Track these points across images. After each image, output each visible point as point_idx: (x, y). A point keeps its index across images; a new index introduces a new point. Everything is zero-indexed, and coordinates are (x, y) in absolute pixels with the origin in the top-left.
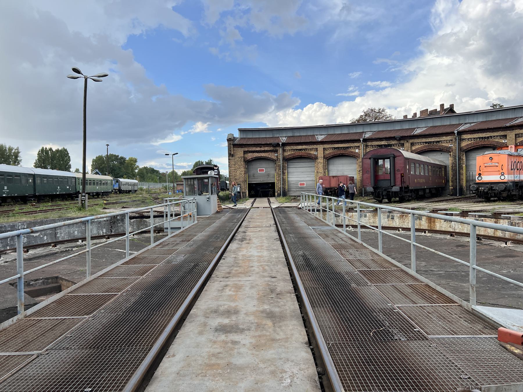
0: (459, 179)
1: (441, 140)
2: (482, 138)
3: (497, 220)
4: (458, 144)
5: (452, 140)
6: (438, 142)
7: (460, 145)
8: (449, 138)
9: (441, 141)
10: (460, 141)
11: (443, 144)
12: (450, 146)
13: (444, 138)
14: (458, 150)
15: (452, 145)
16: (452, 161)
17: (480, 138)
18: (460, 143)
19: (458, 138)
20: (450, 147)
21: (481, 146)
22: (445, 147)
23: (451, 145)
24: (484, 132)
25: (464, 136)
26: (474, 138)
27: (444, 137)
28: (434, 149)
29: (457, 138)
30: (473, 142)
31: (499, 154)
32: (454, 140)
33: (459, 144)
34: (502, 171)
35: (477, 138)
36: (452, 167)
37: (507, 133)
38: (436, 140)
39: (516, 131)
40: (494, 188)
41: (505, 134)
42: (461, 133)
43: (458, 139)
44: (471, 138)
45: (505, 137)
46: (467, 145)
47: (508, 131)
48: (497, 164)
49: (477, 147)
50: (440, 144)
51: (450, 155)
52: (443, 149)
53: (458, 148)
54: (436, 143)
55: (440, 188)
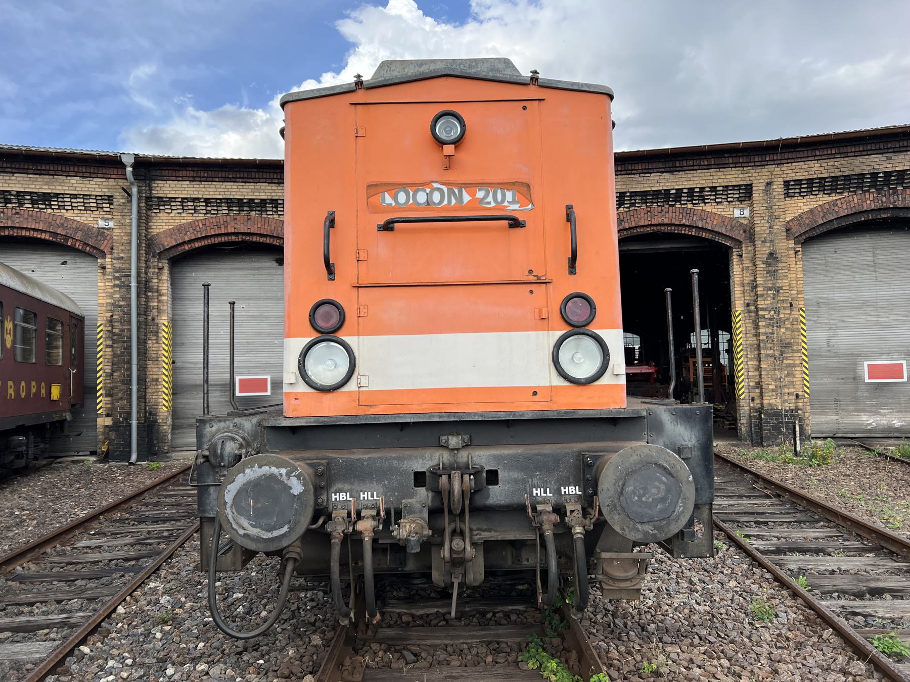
0: (142, 381)
1: (58, 189)
2: (240, 203)
4: (139, 218)
5: (110, 199)
6: (46, 198)
7: (147, 229)
8: (96, 186)
9: (57, 195)
10: (149, 208)
11: (70, 215)
12: (102, 224)
13: (72, 184)
14: (139, 245)
15: (111, 224)
16: (111, 296)
17: (230, 202)
18: (147, 216)
19: (139, 192)
20: (101, 232)
21: (233, 238)
22: (77, 230)
23: (105, 219)
24: (246, 180)
25: (166, 188)
26: (207, 201)
27: (74, 180)
28: (23, 233)
29: (135, 190)
30: (202, 216)
31: (532, 92)
32: (119, 199)
33: (144, 221)
34: (568, 285)
35: (219, 202)
36: (111, 322)
38: (32, 188)
40: (497, 494)
42: (154, 173)
43: (139, 199)
44: (194, 200)
46: (179, 229)
48: (510, 203)
49: (217, 240)
50: (54, 212)
51: (104, 268)
52: (67, 237)
53: (139, 238)
54: (33, 202)
55: (21, 430)
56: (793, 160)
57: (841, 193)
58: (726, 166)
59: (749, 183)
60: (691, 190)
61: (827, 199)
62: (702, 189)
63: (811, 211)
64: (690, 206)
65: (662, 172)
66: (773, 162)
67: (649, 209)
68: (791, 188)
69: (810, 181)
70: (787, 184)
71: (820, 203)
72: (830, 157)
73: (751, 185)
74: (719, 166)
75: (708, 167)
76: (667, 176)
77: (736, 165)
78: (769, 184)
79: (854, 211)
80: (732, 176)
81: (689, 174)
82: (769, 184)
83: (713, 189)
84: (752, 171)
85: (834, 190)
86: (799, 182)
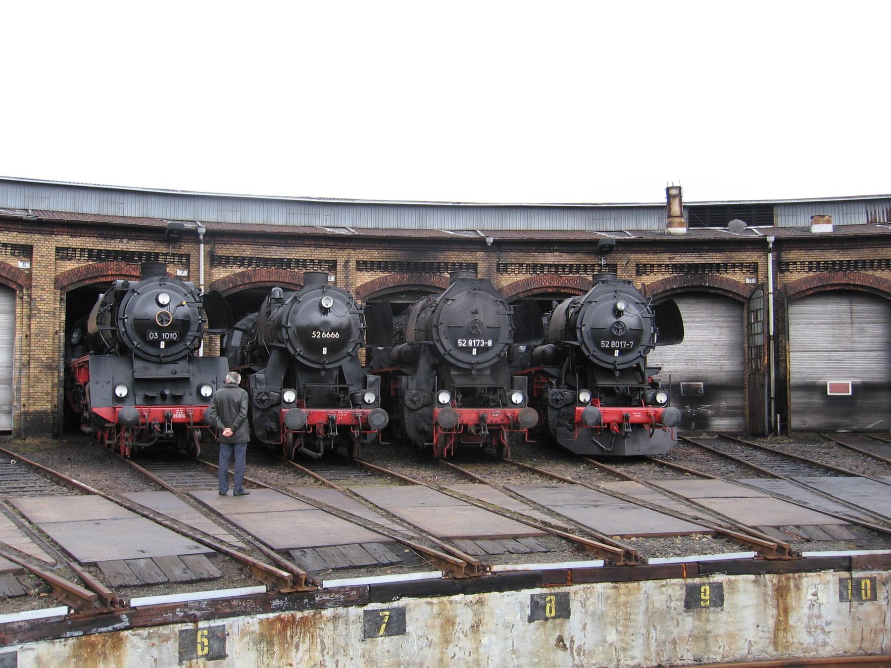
3: (788, 579)
37: (37, 241)
39: (60, 238)
41: (29, 242)
45: (26, 251)
47: (38, 236)
56: (362, 248)
57: (390, 272)
58: (321, 246)
59: (335, 259)
60: (297, 261)
61: (382, 275)
62: (305, 261)
63: (372, 281)
64: (296, 270)
65: (279, 246)
66: (349, 247)
67: (269, 270)
68: (362, 266)
69: (372, 263)
70: (358, 262)
71: (378, 277)
72: (384, 249)
73: (336, 261)
74: (316, 246)
75: (309, 246)
76: (282, 249)
77: (327, 246)
78: (347, 262)
79: (397, 285)
80: (324, 254)
81: (297, 249)
82: (347, 262)
83: (312, 261)
84: (338, 252)
85: (385, 269)
86: (365, 262)
